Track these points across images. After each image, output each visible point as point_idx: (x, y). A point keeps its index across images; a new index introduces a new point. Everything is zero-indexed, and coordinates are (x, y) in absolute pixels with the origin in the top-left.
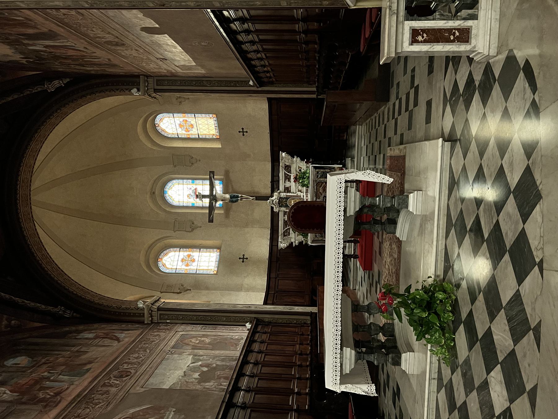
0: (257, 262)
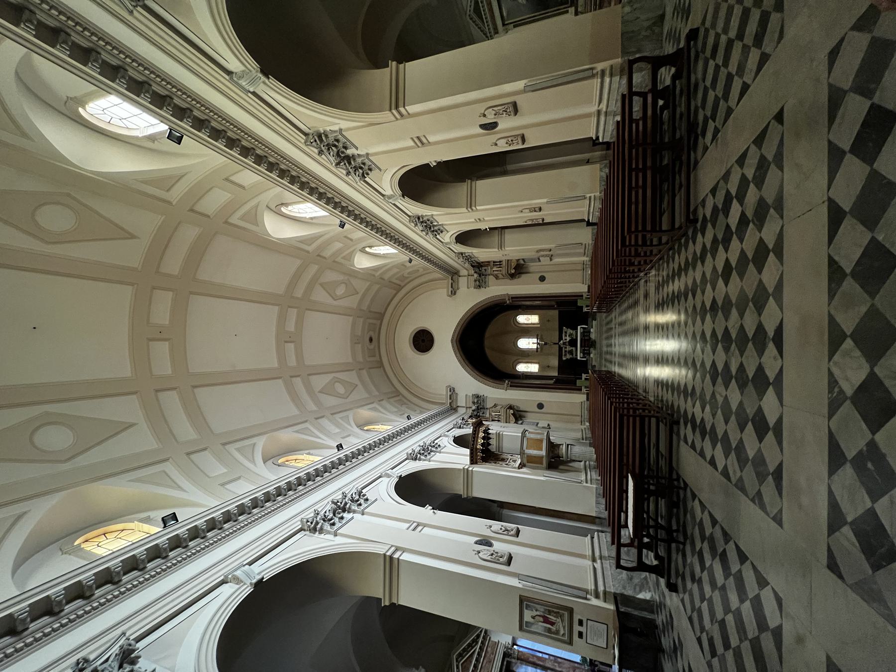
0: (553, 368)
